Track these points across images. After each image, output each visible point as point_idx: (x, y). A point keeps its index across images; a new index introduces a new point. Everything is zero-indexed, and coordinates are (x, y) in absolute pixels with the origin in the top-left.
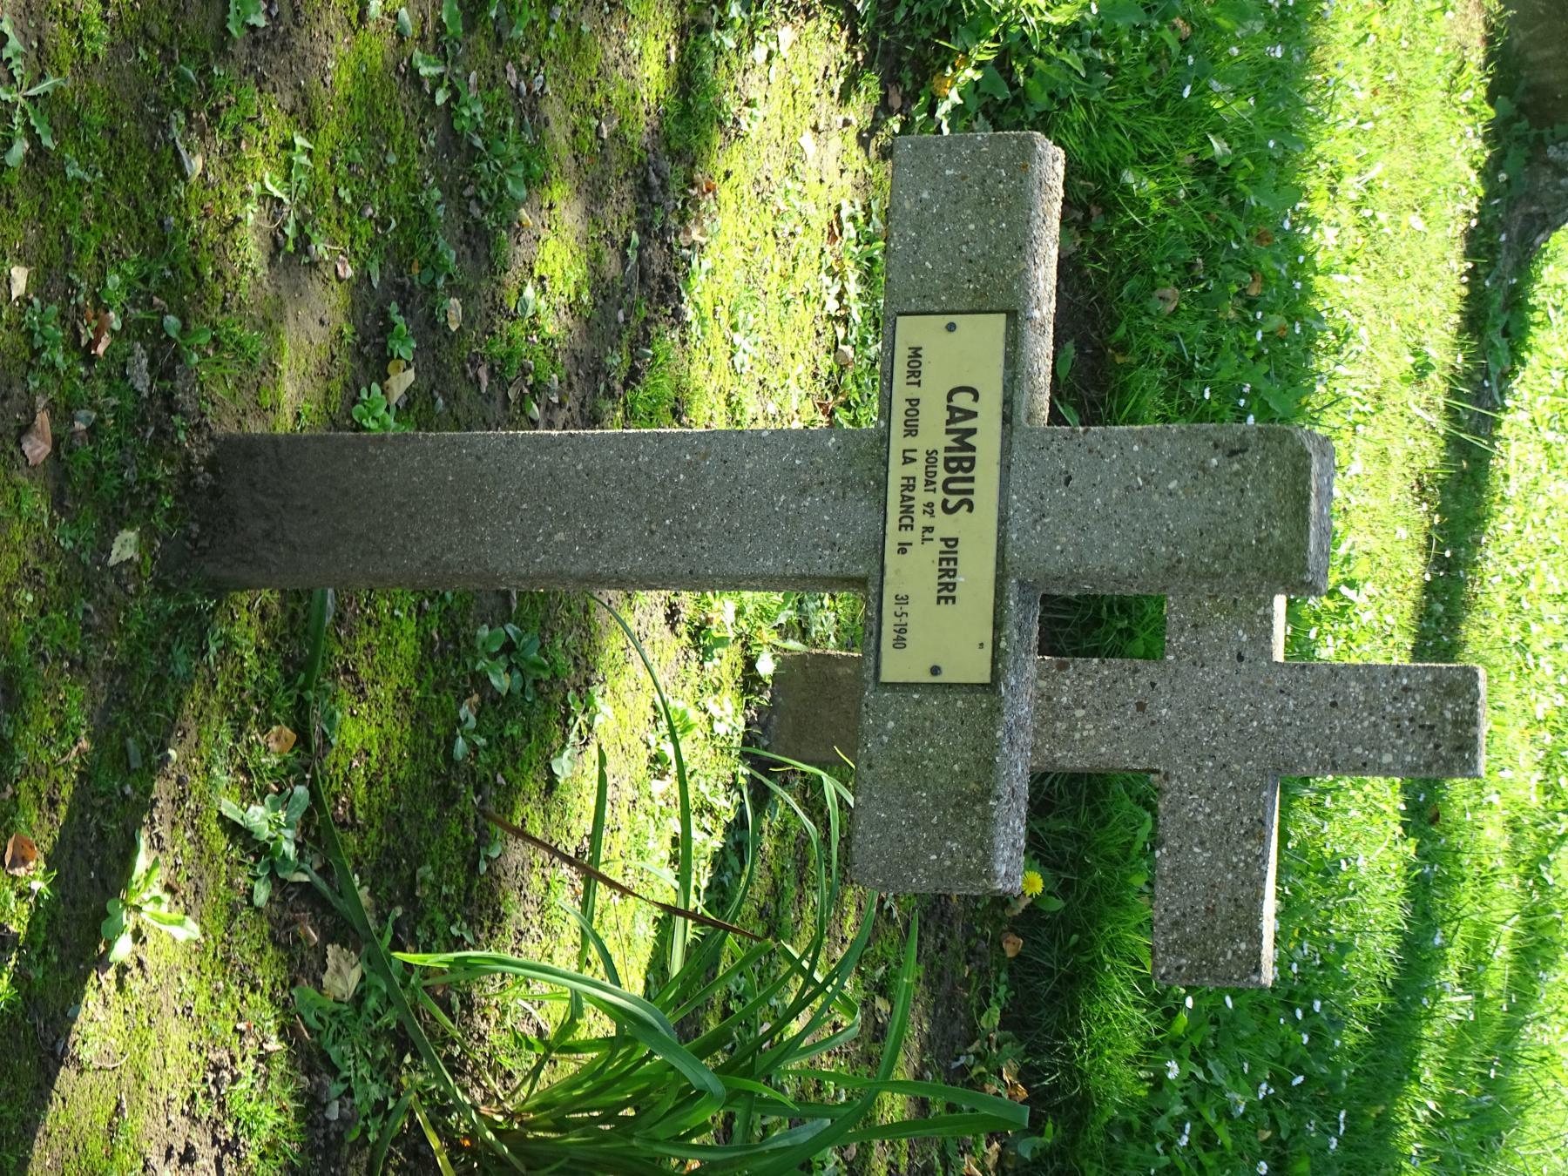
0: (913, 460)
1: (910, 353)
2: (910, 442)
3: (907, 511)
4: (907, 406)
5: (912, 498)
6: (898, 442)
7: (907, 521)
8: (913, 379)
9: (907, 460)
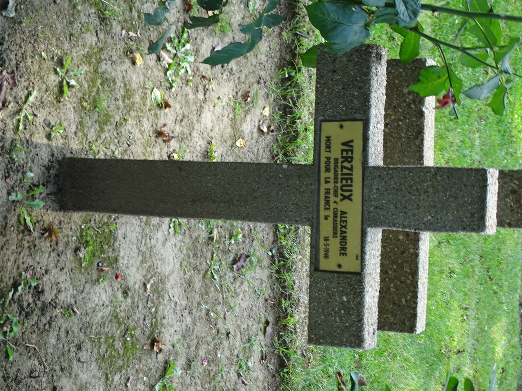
0: (329, 182)
1: (326, 139)
2: (328, 175)
3: (327, 202)
4: (326, 160)
5: (329, 197)
6: (323, 175)
7: (327, 206)
8: (328, 150)
9: (327, 182)
